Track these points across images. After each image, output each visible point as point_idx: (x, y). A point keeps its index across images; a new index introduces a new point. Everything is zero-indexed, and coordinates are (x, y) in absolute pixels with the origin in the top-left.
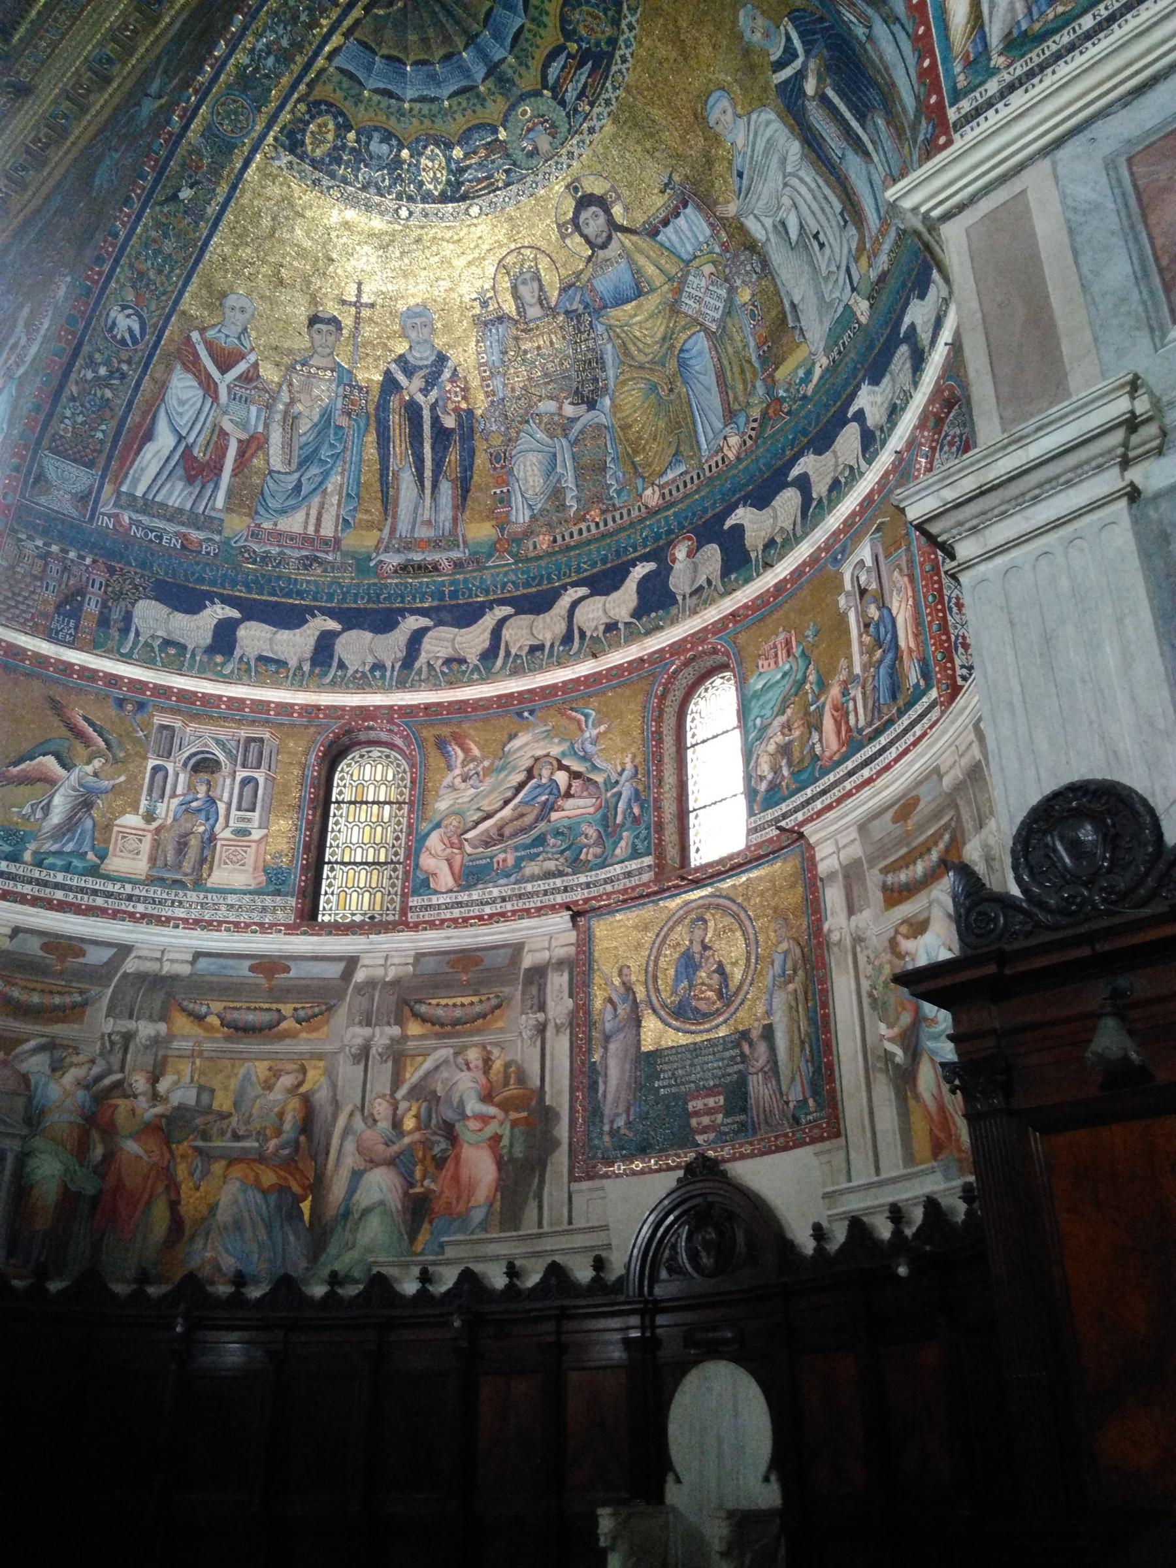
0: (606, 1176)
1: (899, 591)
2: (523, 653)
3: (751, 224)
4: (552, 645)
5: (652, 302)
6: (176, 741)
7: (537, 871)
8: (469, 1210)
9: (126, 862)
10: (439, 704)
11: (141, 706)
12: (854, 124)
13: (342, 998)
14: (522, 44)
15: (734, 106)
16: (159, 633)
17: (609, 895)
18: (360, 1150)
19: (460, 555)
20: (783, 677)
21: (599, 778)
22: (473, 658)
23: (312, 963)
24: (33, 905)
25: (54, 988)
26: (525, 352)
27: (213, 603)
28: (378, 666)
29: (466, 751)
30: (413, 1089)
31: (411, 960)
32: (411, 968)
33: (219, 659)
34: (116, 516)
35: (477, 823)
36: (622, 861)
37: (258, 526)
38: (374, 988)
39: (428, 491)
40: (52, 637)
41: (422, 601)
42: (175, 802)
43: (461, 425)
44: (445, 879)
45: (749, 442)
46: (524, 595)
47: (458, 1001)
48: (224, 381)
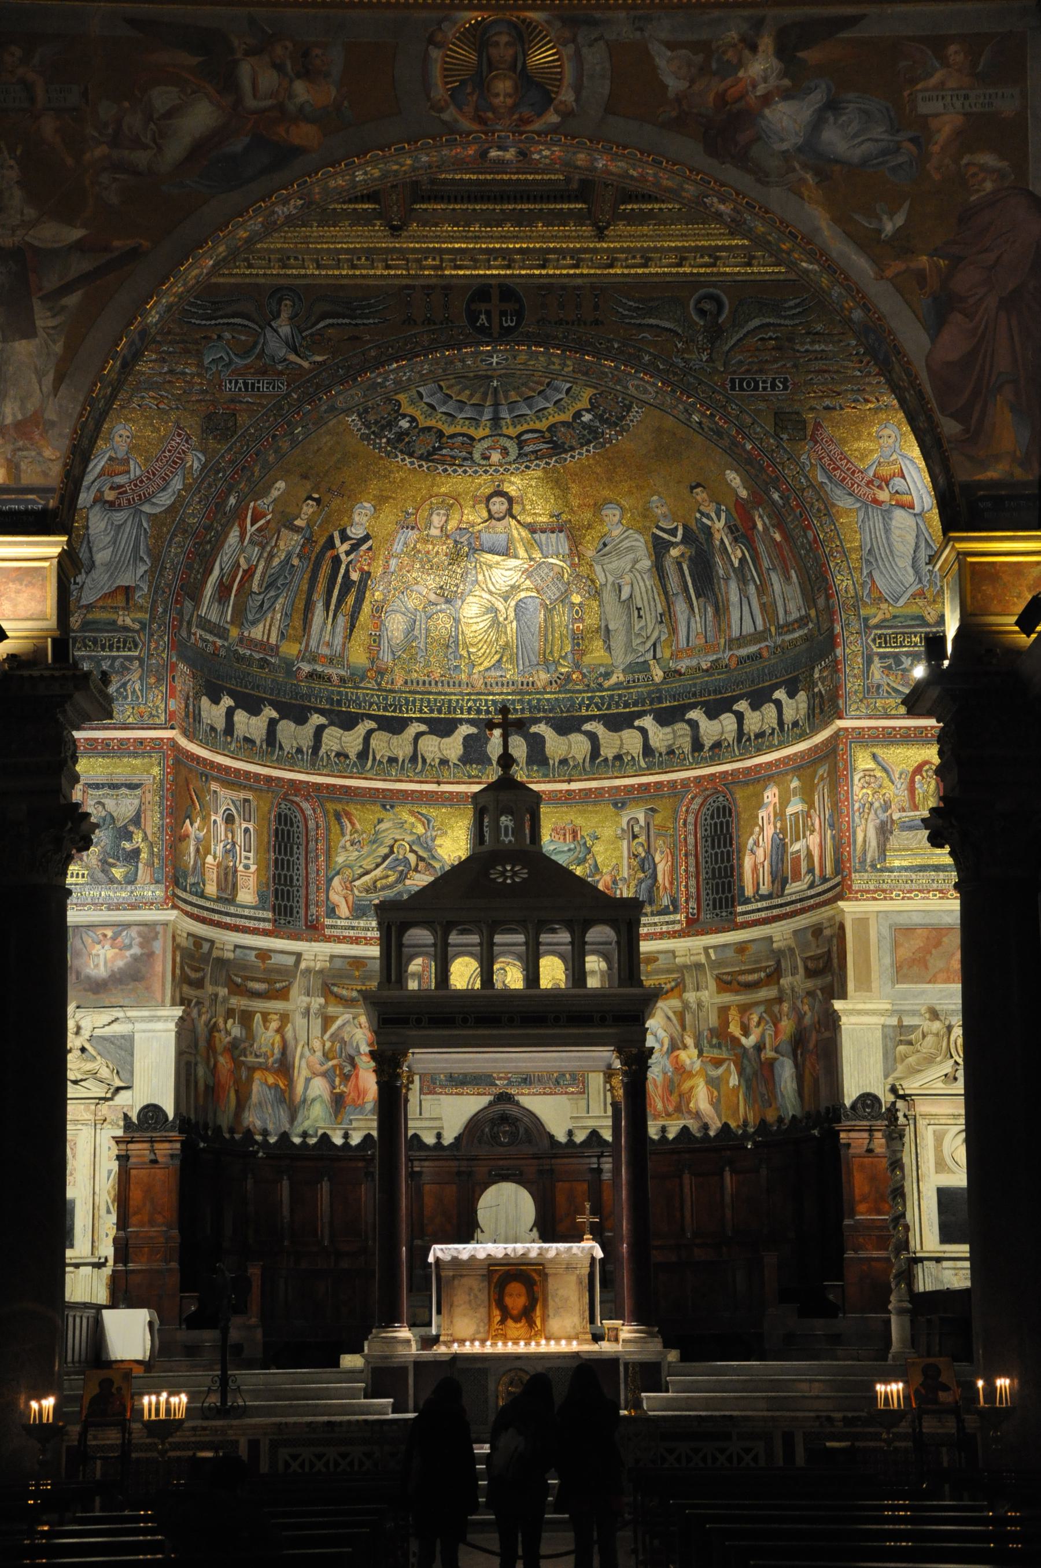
0: (441, 1093)
1: (662, 852)
3: (598, 568)
4: (403, 761)
5: (512, 563)
8: (364, 1103)
10: (334, 786)
12: (692, 591)
13: (295, 977)
14: (522, 420)
15: (622, 518)
18: (308, 1066)
20: (570, 850)
21: (437, 865)
22: (353, 756)
26: (419, 551)
28: (299, 750)
29: (353, 824)
30: (332, 1035)
38: (310, 972)
39: (330, 620)
42: (222, 845)
43: (360, 581)
44: (344, 910)
45: (554, 685)
48: (251, 529)
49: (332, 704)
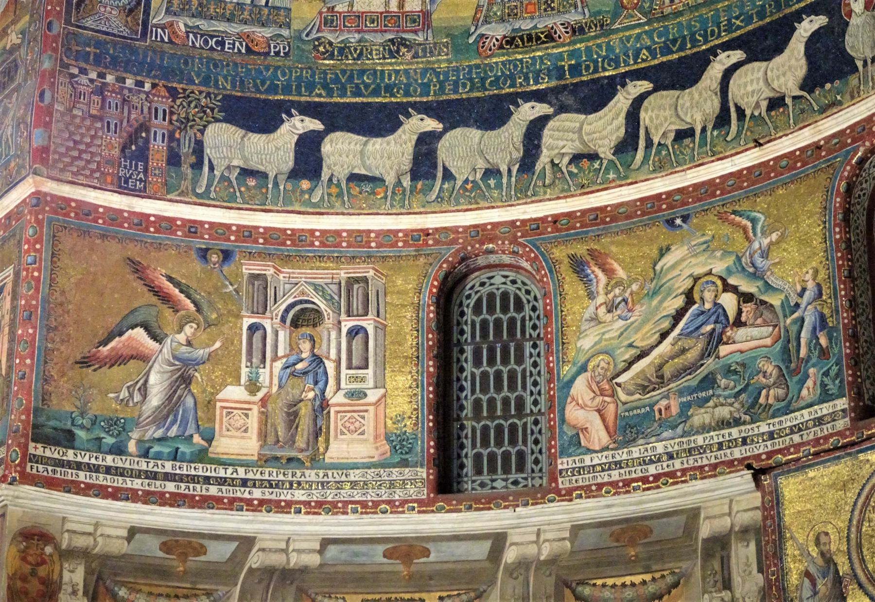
2: (669, 142)
4: (704, 130)
6: (271, 292)
7: (707, 419)
9: (235, 441)
10: (570, 215)
11: (227, 255)
13: (492, 582)
16: (235, 163)
17: (797, 446)
19: (578, 17)
21: (775, 301)
22: (606, 152)
23: (454, 544)
24: (145, 503)
25: (180, 592)
27: (291, 115)
28: (491, 172)
29: (609, 272)
31: (567, 534)
32: (568, 544)
33: (305, 184)
34: (171, 24)
35: (630, 364)
36: (811, 405)
37: (331, 9)
38: (528, 569)
40: (123, 187)
41: (536, 82)
42: (279, 365)
44: (598, 435)
46: (662, 63)
47: (628, 580)
49: (561, 77)
